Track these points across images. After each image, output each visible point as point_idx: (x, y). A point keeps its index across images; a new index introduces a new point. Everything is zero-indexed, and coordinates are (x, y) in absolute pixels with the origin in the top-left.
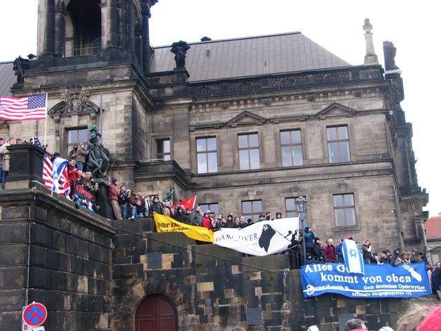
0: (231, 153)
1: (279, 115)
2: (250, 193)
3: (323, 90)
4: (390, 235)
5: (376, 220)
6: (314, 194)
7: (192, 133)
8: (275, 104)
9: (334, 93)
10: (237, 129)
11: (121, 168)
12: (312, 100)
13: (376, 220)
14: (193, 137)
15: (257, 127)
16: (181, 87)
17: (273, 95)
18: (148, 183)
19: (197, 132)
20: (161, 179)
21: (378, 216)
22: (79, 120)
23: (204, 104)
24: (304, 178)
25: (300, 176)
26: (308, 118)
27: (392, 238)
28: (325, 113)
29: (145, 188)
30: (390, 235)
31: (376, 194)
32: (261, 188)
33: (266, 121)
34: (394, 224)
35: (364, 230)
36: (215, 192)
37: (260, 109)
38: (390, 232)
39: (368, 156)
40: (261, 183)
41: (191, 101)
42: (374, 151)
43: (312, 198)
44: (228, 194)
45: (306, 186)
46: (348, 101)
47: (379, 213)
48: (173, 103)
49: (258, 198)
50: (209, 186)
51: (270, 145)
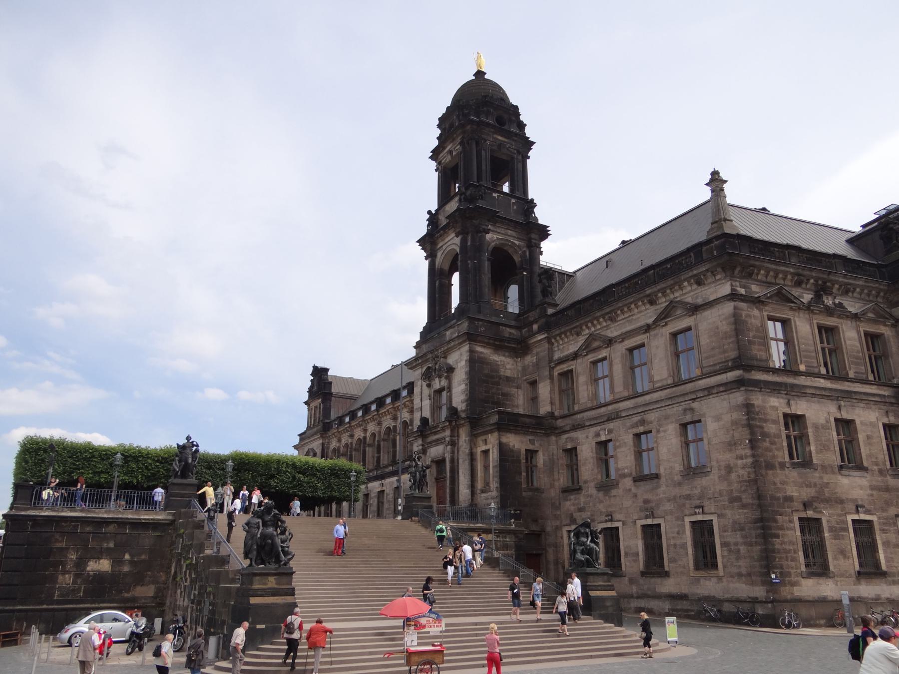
0: (585, 387)
1: (624, 330)
2: (601, 433)
3: (659, 287)
4: (746, 478)
5: (727, 457)
6: (660, 425)
7: (555, 370)
9: (671, 288)
10: (589, 357)
11: (463, 425)
12: (652, 303)
13: (727, 457)
14: (556, 374)
15: (606, 350)
16: (543, 320)
17: (613, 308)
18: (483, 438)
19: (558, 368)
20: (491, 432)
21: (730, 450)
22: (440, 381)
23: (560, 335)
24: (647, 408)
25: (644, 405)
26: (648, 328)
27: (749, 482)
28: (664, 318)
29: (481, 443)
30: (746, 478)
31: (727, 418)
32: (611, 425)
33: (610, 342)
34: (750, 460)
35: (715, 471)
36: (573, 434)
38: (744, 473)
39: (715, 365)
40: (610, 419)
41: (546, 335)
42: (722, 356)
43: (658, 431)
44: (584, 436)
45: (652, 417)
46: (690, 294)
47: (731, 445)
48: (535, 340)
49: (608, 438)
50: (568, 428)
51: (618, 370)
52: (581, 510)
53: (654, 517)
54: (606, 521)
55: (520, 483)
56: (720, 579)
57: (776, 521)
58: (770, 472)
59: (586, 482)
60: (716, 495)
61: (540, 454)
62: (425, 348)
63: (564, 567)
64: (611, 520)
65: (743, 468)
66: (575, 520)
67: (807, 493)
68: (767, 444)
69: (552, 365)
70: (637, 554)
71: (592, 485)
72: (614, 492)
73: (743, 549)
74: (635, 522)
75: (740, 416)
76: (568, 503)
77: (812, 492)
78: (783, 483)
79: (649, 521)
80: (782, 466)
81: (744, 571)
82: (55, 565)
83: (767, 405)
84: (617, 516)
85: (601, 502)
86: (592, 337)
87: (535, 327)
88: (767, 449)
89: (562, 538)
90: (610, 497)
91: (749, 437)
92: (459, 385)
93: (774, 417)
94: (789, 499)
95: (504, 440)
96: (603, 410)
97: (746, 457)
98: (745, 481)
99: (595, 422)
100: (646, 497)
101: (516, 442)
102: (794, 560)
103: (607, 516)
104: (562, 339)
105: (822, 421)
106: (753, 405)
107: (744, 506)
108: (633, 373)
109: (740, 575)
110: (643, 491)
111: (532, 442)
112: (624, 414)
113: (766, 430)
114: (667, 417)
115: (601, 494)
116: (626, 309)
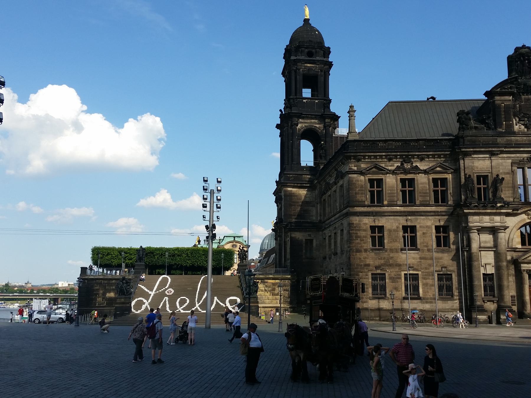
57: (358, 275)
58: (358, 254)
61: (314, 241)
67: (378, 262)
68: (358, 241)
77: (382, 262)
80: (366, 250)
82: (96, 295)
83: (362, 223)
88: (358, 243)
93: (364, 227)
94: (369, 265)
95: (293, 235)
101: (299, 236)
105: (394, 227)
106: (353, 224)
111: (310, 235)
113: (359, 234)
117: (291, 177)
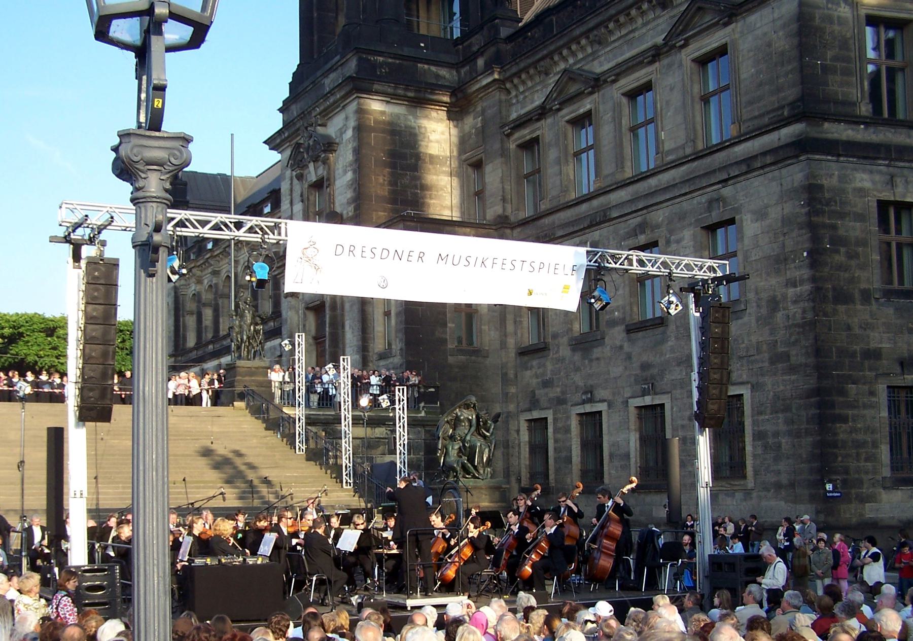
6: (671, 232)
8: (615, 37)
14: (513, 146)
17: (600, 19)
19: (517, 135)
21: (778, 272)
25: (647, 196)
26: (656, 54)
30: (799, 320)
31: (775, 213)
33: (597, 83)
34: (807, 287)
35: (752, 309)
37: (594, 56)
38: (795, 310)
39: (762, 116)
42: (774, 98)
43: (668, 242)
45: (659, 216)
47: (779, 261)
48: (477, 86)
52: (547, 384)
53: (656, 394)
54: (584, 402)
55: (444, 341)
56: (748, 493)
57: (843, 392)
58: (842, 308)
59: (555, 336)
60: (751, 352)
62: (295, 110)
63: (519, 480)
64: (591, 401)
65: (795, 302)
66: (538, 401)
68: (840, 258)
69: (507, 130)
70: (627, 456)
71: (564, 340)
72: (597, 352)
73: (784, 441)
74: (626, 403)
75: (795, 208)
76: (528, 373)
78: (866, 326)
79: (648, 400)
80: (866, 296)
81: (784, 479)
83: (849, 187)
84: (601, 393)
85: (577, 369)
86: (569, 75)
87: (480, 62)
88: (840, 267)
89: (518, 431)
90: (591, 361)
91: (807, 245)
92: (345, 172)
93: (858, 209)
94: (874, 355)
96: (584, 207)
97: (802, 282)
98: (797, 325)
99: (571, 230)
100: (645, 358)
102: (871, 458)
103: (585, 393)
104: (524, 83)
106: (821, 187)
107: (793, 369)
108: (636, 136)
109: (778, 486)
110: (641, 349)
112: (615, 214)
113: (841, 232)
114: (682, 216)
115: (577, 357)
116: (622, 19)
117: (381, 65)
